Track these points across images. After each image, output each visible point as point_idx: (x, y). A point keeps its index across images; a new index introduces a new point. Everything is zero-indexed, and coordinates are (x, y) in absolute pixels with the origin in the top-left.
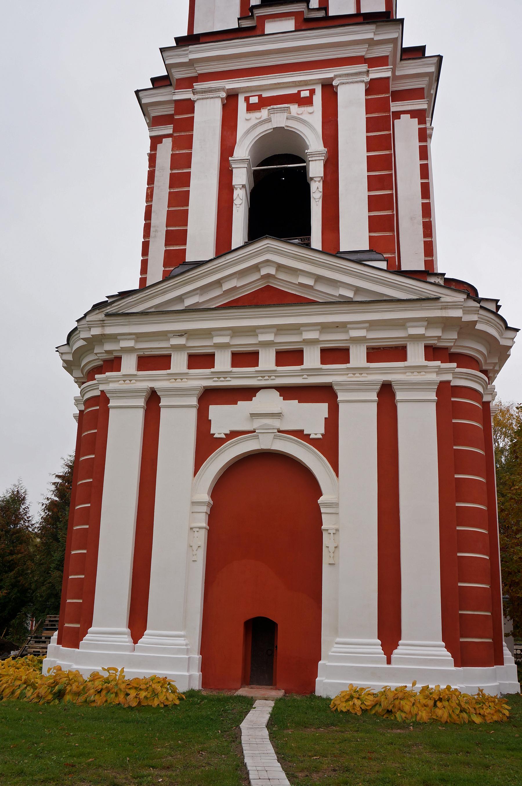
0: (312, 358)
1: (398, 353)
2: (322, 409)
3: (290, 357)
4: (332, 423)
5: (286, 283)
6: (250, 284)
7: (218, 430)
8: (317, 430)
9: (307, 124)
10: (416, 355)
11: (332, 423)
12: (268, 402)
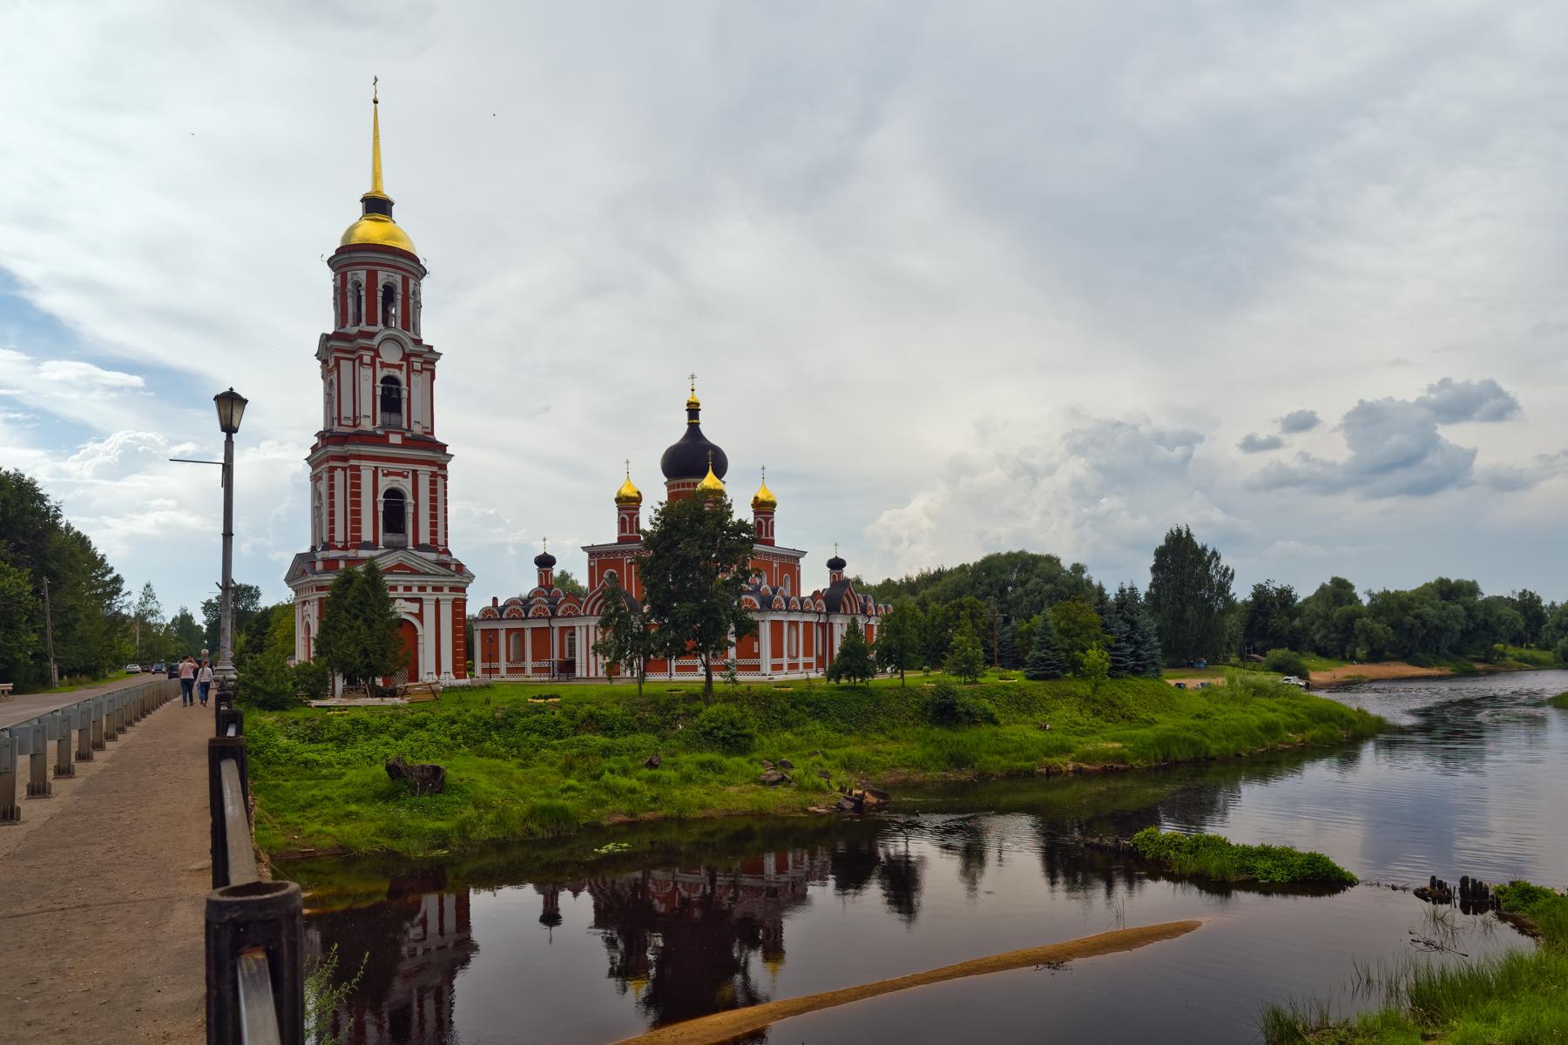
0: (415, 590)
1: (440, 589)
4: (421, 609)
5: (407, 563)
9: (406, 485)
10: (446, 590)
11: (421, 609)
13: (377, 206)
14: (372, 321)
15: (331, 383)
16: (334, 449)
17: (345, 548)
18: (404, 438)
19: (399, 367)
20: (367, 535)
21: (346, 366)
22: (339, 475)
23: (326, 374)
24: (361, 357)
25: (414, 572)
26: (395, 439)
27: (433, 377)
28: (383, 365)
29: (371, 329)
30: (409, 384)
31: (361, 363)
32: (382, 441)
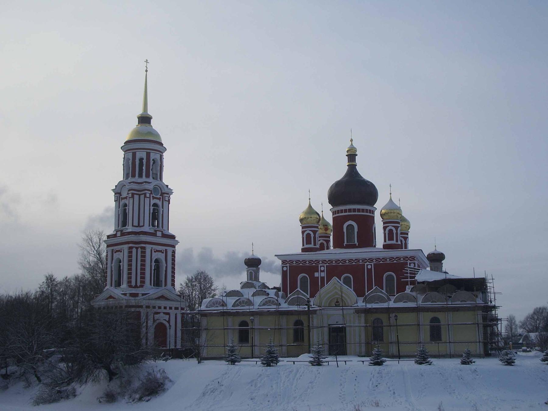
2: (168, 316)
3: (165, 308)
6: (160, 294)
7: (156, 318)
8: (167, 320)
9: (161, 256)
12: (162, 314)
13: (145, 120)
15: (125, 205)
17: (136, 286)
18: (162, 234)
19: (159, 199)
21: (136, 197)
22: (134, 250)
24: (145, 194)
25: (167, 299)
26: (159, 234)
27: (169, 203)
28: (154, 198)
29: (147, 180)
30: (163, 208)
31: (145, 197)
32: (154, 234)
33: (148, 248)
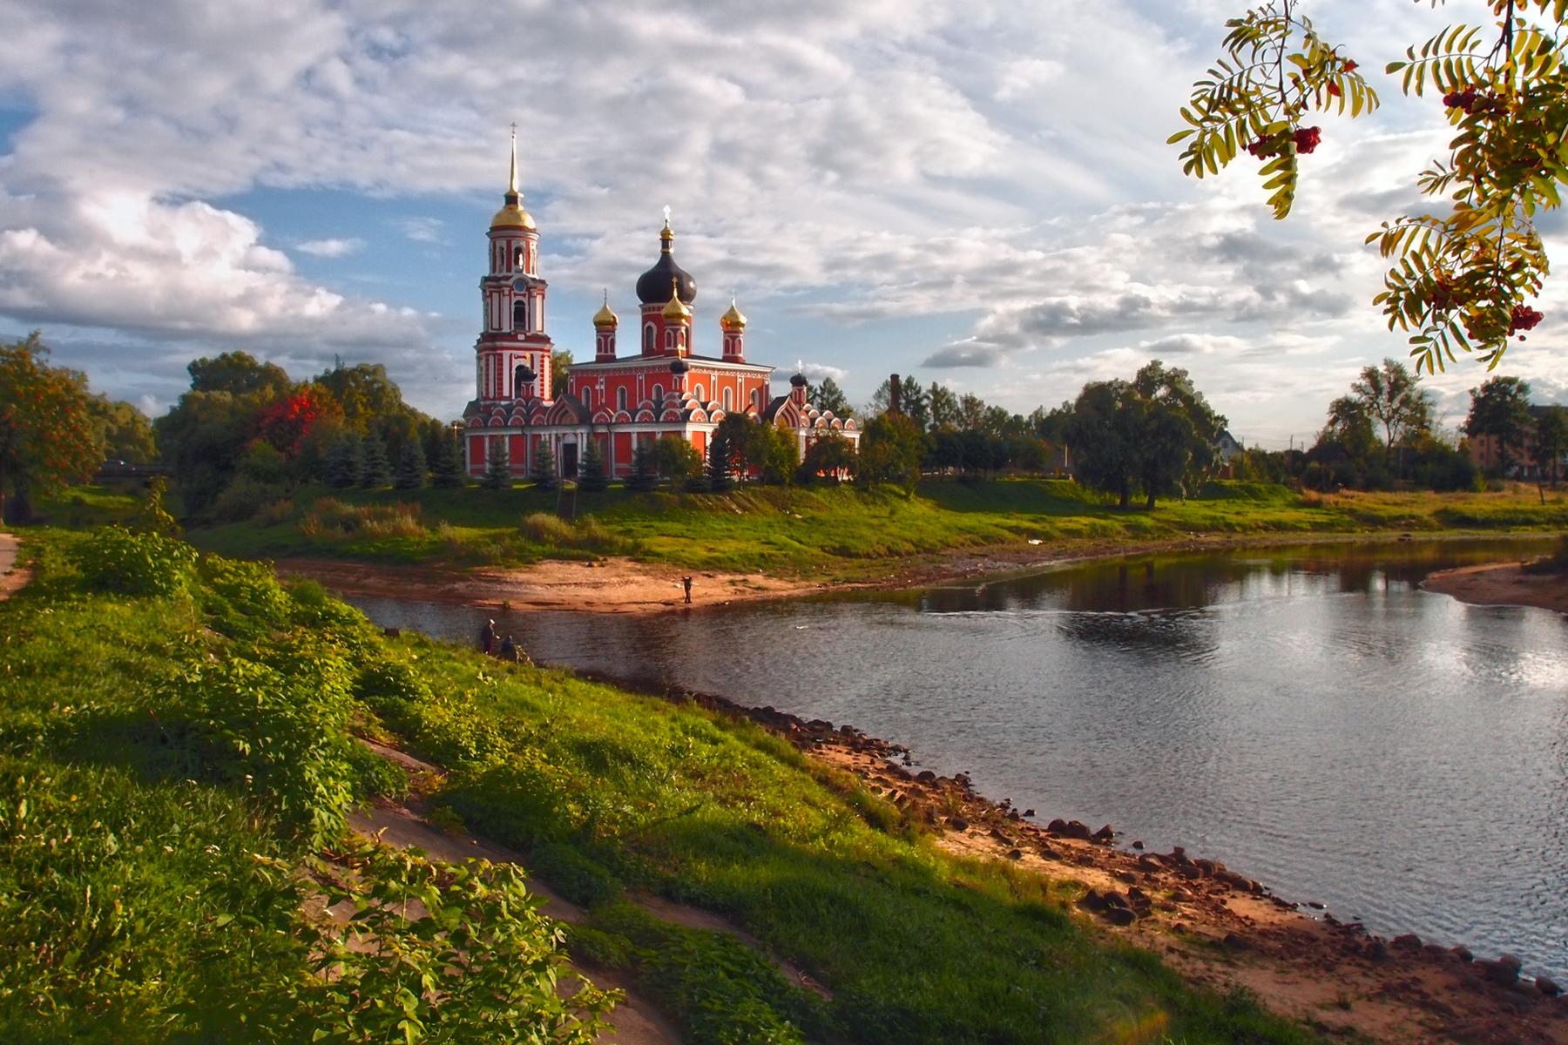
14: (509, 270)
16: (488, 344)
20: (506, 393)
21: (495, 295)
22: (491, 358)
23: (485, 298)
33: (506, 354)
